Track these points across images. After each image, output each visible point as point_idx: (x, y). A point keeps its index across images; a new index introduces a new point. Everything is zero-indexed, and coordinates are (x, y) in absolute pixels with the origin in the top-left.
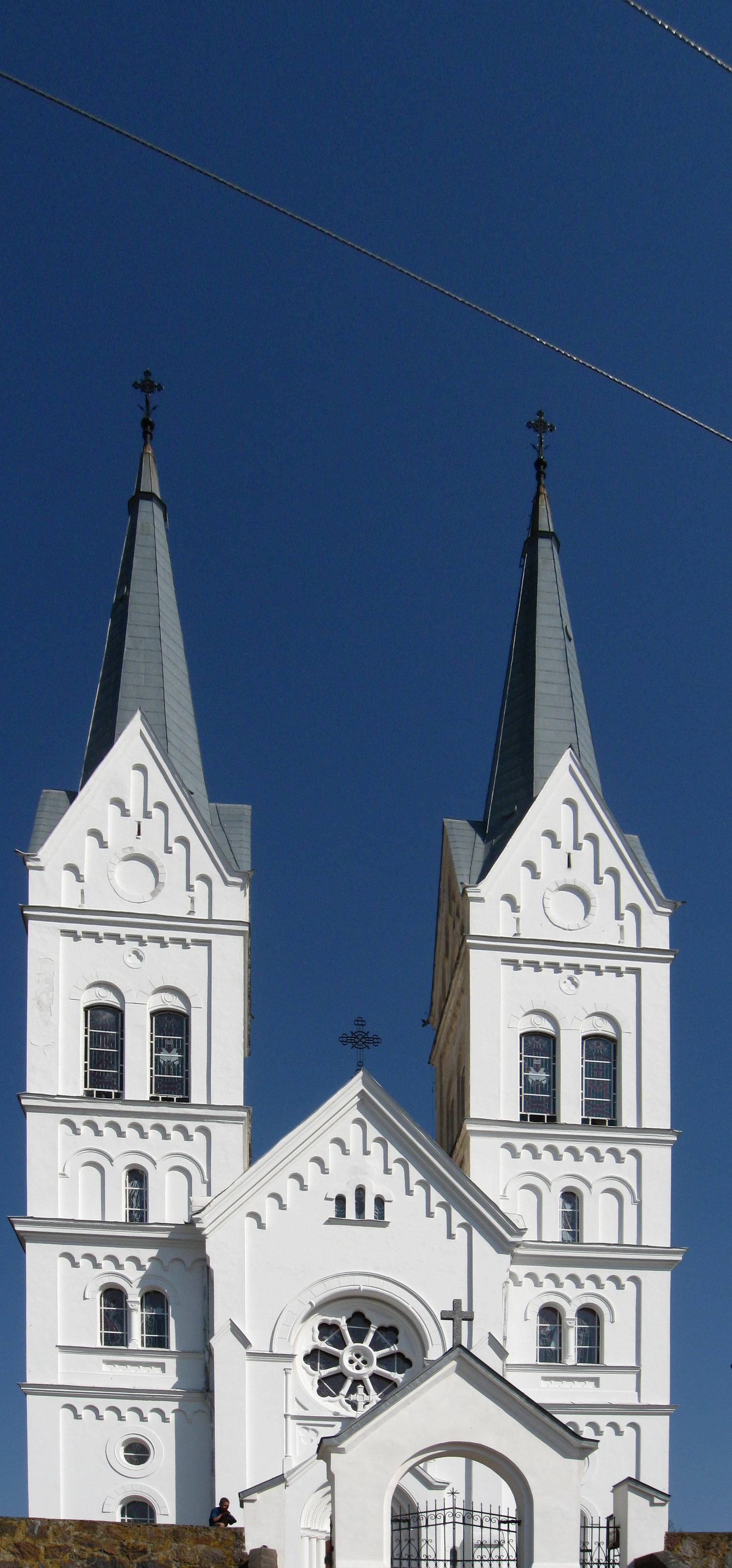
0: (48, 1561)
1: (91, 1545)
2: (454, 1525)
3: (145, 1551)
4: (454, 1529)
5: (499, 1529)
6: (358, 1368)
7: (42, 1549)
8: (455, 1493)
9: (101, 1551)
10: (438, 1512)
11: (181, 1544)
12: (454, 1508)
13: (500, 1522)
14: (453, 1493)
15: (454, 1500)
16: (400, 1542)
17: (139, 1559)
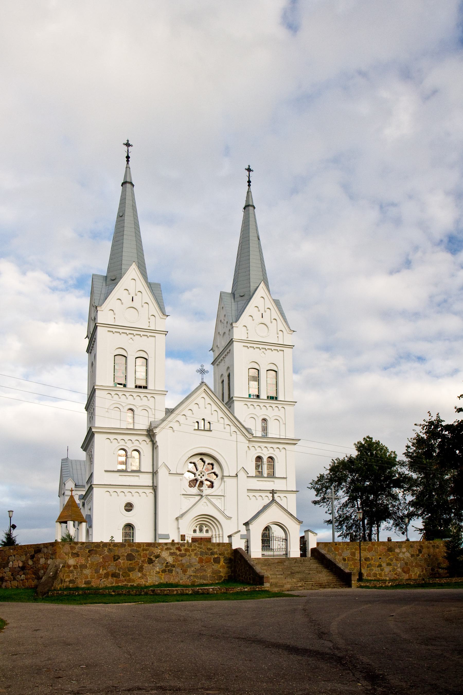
0: (192, 553)
1: (201, 548)
5: (282, 541)
6: (201, 477)
7: (191, 550)
13: (283, 540)
17: (211, 551)
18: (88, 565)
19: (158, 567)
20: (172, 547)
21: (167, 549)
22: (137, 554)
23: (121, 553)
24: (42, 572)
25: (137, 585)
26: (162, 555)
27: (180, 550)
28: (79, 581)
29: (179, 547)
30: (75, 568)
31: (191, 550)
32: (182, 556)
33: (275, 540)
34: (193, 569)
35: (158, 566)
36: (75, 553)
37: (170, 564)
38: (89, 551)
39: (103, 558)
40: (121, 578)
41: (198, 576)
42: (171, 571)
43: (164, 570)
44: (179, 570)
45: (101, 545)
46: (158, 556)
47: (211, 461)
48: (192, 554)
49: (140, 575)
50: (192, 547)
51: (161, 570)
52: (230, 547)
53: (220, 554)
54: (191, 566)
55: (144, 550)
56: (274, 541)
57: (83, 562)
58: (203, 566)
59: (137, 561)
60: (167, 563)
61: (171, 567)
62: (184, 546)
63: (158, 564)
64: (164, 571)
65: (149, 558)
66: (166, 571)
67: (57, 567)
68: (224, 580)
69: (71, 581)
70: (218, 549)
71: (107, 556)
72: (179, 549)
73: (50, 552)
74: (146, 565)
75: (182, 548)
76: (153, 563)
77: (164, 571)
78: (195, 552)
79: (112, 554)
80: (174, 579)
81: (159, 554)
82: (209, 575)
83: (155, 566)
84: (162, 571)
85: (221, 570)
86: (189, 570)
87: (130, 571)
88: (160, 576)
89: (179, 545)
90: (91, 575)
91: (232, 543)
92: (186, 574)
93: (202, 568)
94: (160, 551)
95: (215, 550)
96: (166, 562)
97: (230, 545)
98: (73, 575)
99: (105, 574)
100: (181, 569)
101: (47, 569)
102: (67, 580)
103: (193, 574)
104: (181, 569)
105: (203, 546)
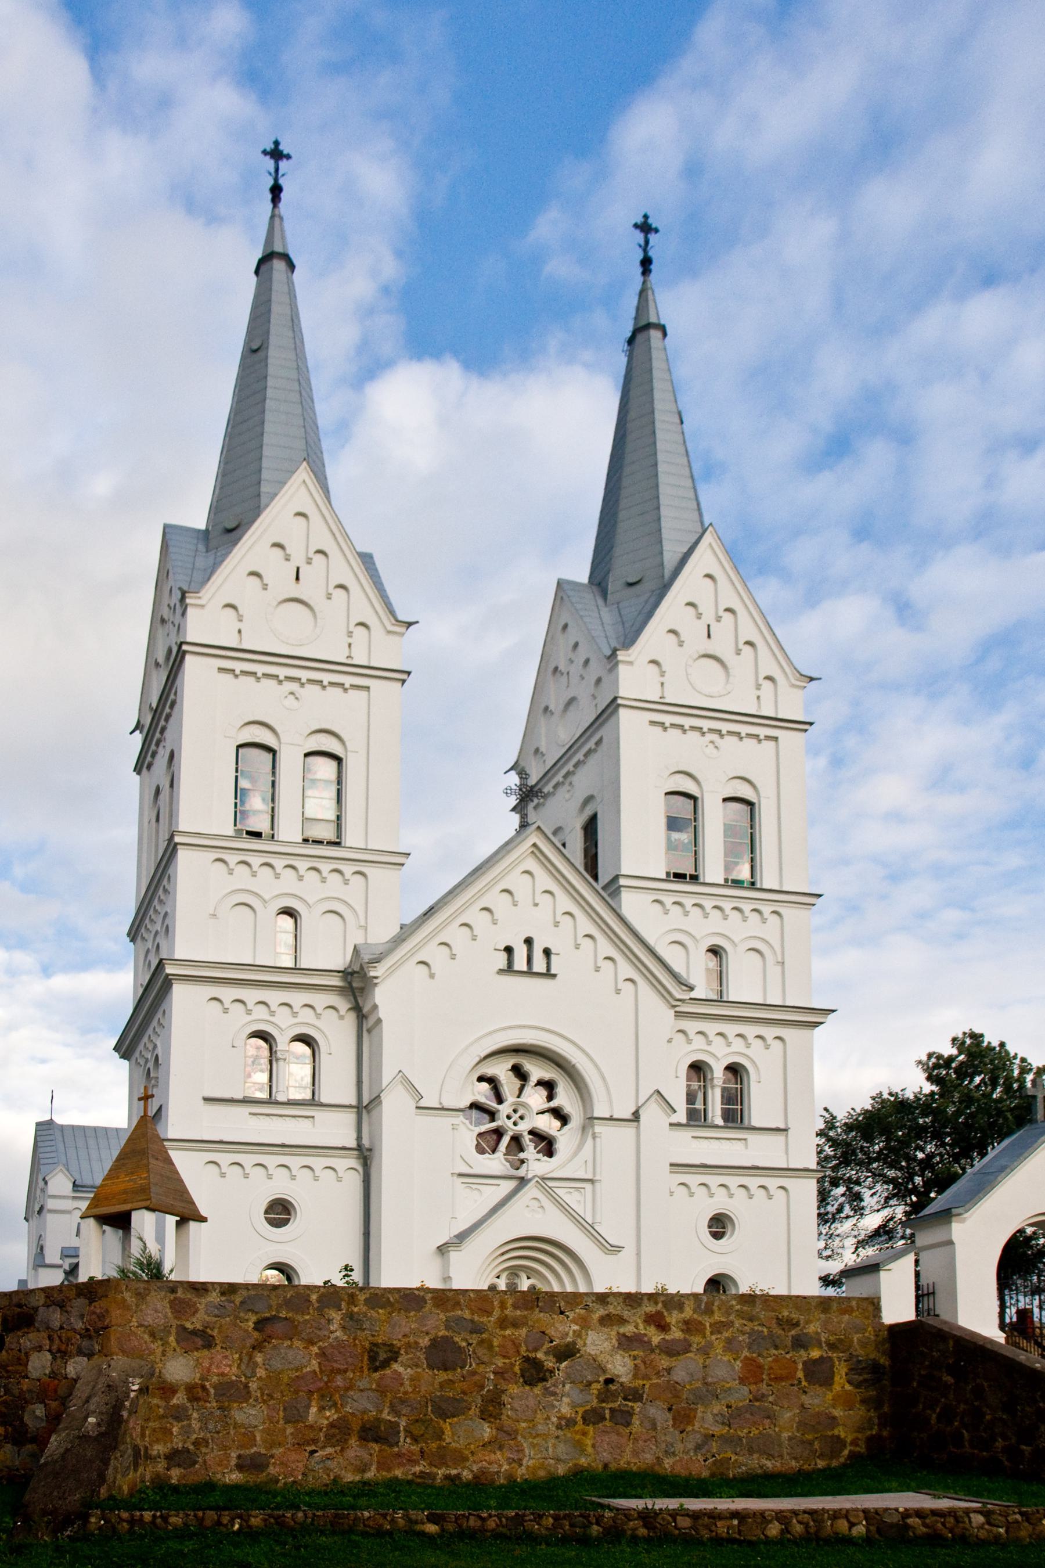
0: (714, 1337)
1: (751, 1320)
3: (797, 1324)
7: (708, 1325)
9: (759, 1324)
11: (828, 1315)
17: (793, 1332)
18: (253, 1386)
19: (565, 1400)
20: (626, 1314)
21: (607, 1320)
22: (474, 1339)
23: (405, 1336)
24: (40, 1410)
25: (475, 1477)
26: (585, 1345)
27: (663, 1327)
28: (211, 1455)
29: (659, 1314)
30: (193, 1398)
31: (708, 1325)
32: (671, 1350)
34: (717, 1408)
35: (568, 1395)
36: (194, 1333)
37: (622, 1384)
38: (260, 1325)
39: (323, 1354)
40: (405, 1444)
41: (740, 1439)
42: (623, 1418)
43: (594, 1410)
44: (658, 1412)
45: (314, 1297)
46: (567, 1352)
48: (716, 1343)
49: (487, 1431)
50: (712, 1312)
51: (581, 1411)
52: (874, 1317)
53: (832, 1346)
54: (710, 1392)
55: (503, 1323)
57: (232, 1372)
58: (763, 1396)
59: (474, 1373)
60: (609, 1381)
61: (625, 1399)
62: (680, 1307)
63: (568, 1386)
64: (593, 1417)
65: (527, 1359)
66: (604, 1419)
67: (116, 1394)
68: (852, 1455)
69: (174, 1457)
70: (825, 1325)
71: (340, 1345)
72: (658, 1322)
73: (79, 1325)
74: (514, 1389)
75: (673, 1318)
76: (544, 1379)
77: (593, 1417)
78: (726, 1334)
79: (365, 1337)
80: (635, 1453)
81: (574, 1343)
82: (785, 1435)
83: (554, 1394)
84: (583, 1418)
85: (837, 1413)
86: (699, 1414)
87: (444, 1415)
88: (578, 1437)
89: (656, 1303)
90: (267, 1432)
91: (879, 1298)
92: (690, 1428)
93: (757, 1404)
94: (576, 1327)
95: (811, 1329)
96: (601, 1379)
97: (871, 1308)
98: (187, 1431)
99: (332, 1425)
100: (670, 1409)
101: (64, 1401)
102: (158, 1449)
103: (718, 1430)
104: (670, 1409)
105: (762, 1309)
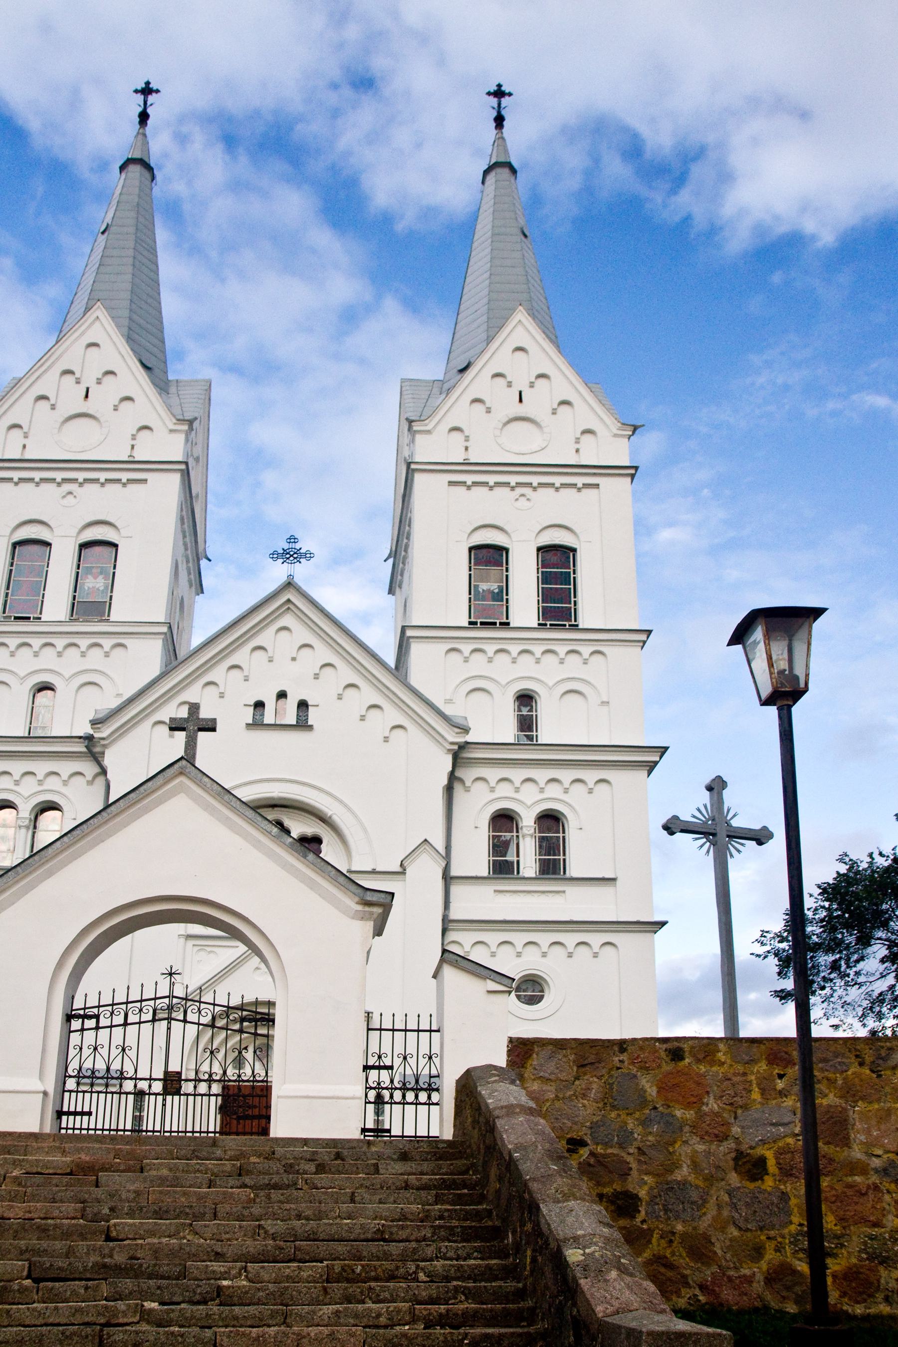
2: (169, 1023)
4: (169, 1029)
8: (174, 973)
10: (144, 1004)
12: (171, 996)
14: (171, 974)
15: (172, 984)
16: (81, 1049)
33: (185, 1021)
47: (307, 828)
56: (176, 1026)
